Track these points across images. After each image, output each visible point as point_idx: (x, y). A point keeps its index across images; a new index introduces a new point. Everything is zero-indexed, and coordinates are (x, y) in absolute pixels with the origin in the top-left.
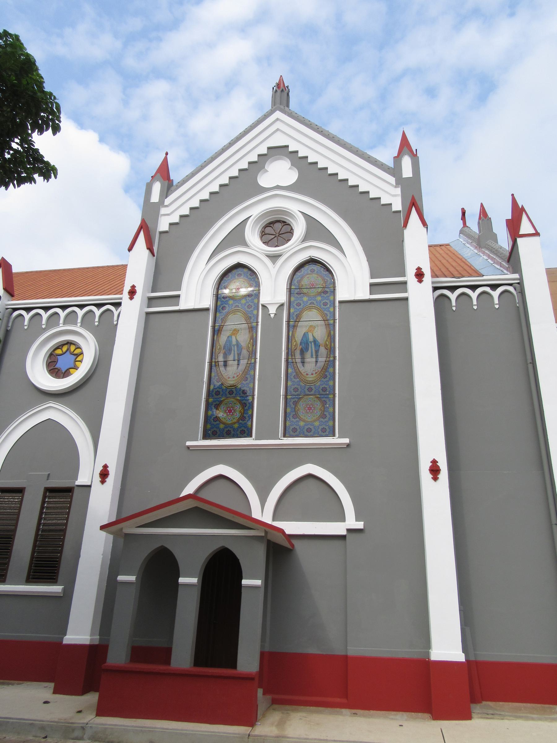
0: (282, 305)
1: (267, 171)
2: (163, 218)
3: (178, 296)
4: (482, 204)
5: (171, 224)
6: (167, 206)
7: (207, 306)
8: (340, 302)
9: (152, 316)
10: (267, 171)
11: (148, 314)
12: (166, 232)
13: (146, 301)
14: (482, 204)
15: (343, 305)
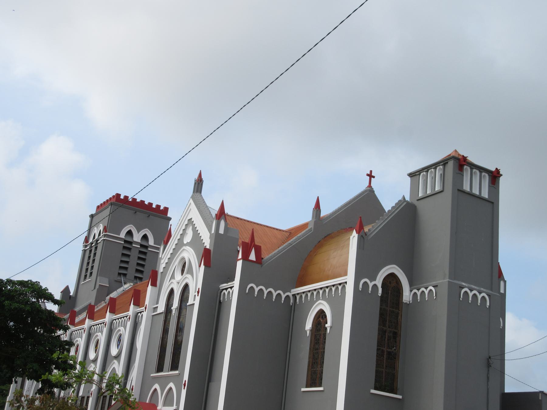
0: (176, 309)
1: (187, 233)
2: (162, 264)
3: (157, 307)
4: (318, 197)
5: (164, 268)
6: (163, 259)
7: (161, 311)
8: (189, 305)
9: (154, 316)
10: (187, 233)
11: (153, 316)
12: (162, 273)
13: (153, 310)
14: (318, 197)
15: (189, 306)
